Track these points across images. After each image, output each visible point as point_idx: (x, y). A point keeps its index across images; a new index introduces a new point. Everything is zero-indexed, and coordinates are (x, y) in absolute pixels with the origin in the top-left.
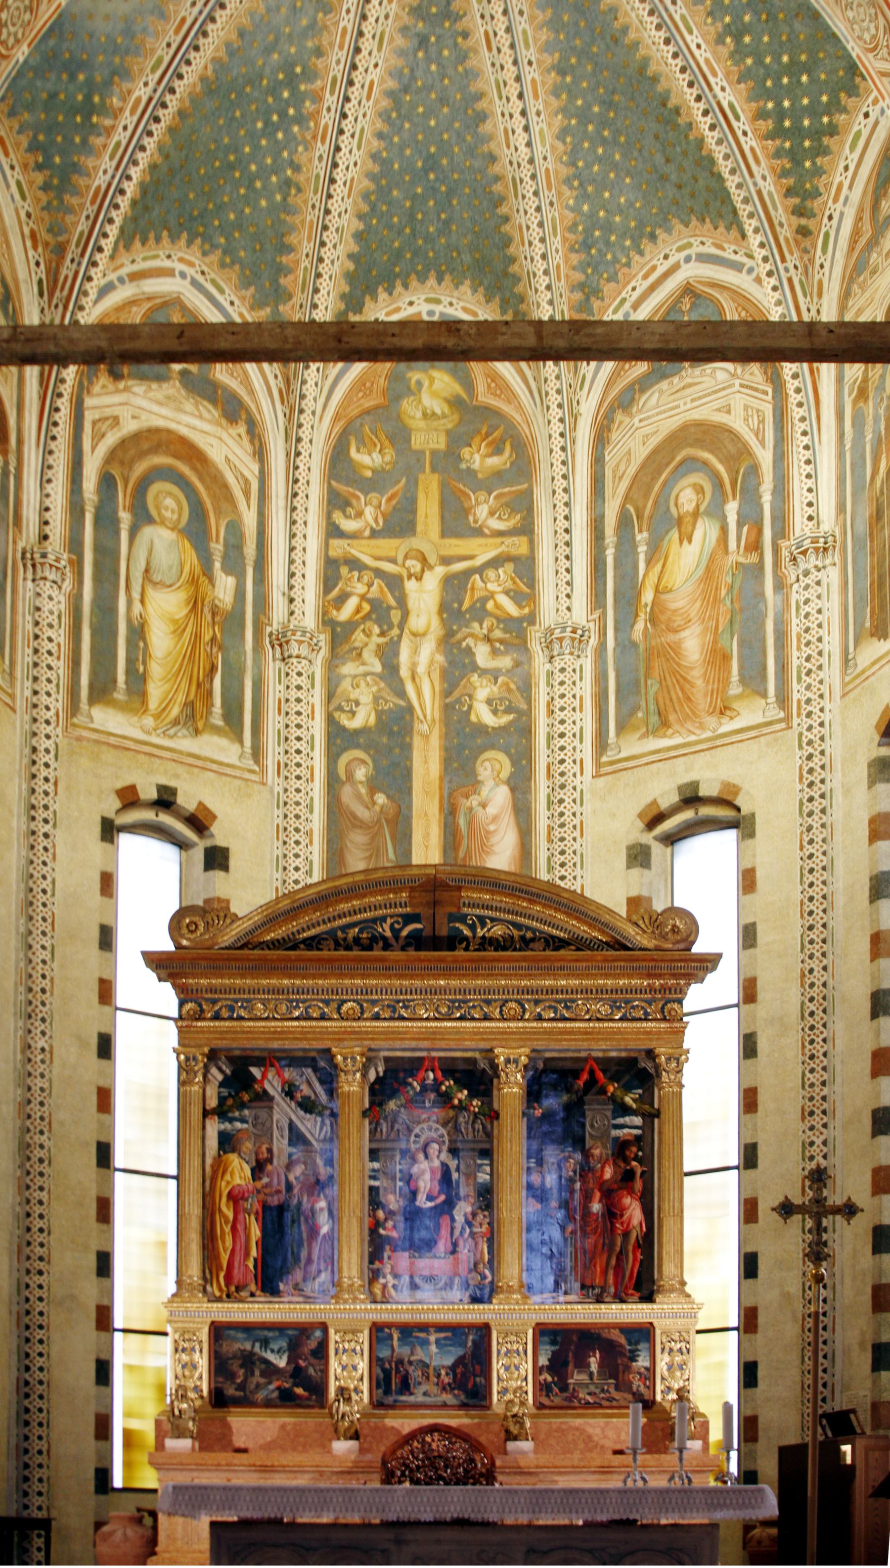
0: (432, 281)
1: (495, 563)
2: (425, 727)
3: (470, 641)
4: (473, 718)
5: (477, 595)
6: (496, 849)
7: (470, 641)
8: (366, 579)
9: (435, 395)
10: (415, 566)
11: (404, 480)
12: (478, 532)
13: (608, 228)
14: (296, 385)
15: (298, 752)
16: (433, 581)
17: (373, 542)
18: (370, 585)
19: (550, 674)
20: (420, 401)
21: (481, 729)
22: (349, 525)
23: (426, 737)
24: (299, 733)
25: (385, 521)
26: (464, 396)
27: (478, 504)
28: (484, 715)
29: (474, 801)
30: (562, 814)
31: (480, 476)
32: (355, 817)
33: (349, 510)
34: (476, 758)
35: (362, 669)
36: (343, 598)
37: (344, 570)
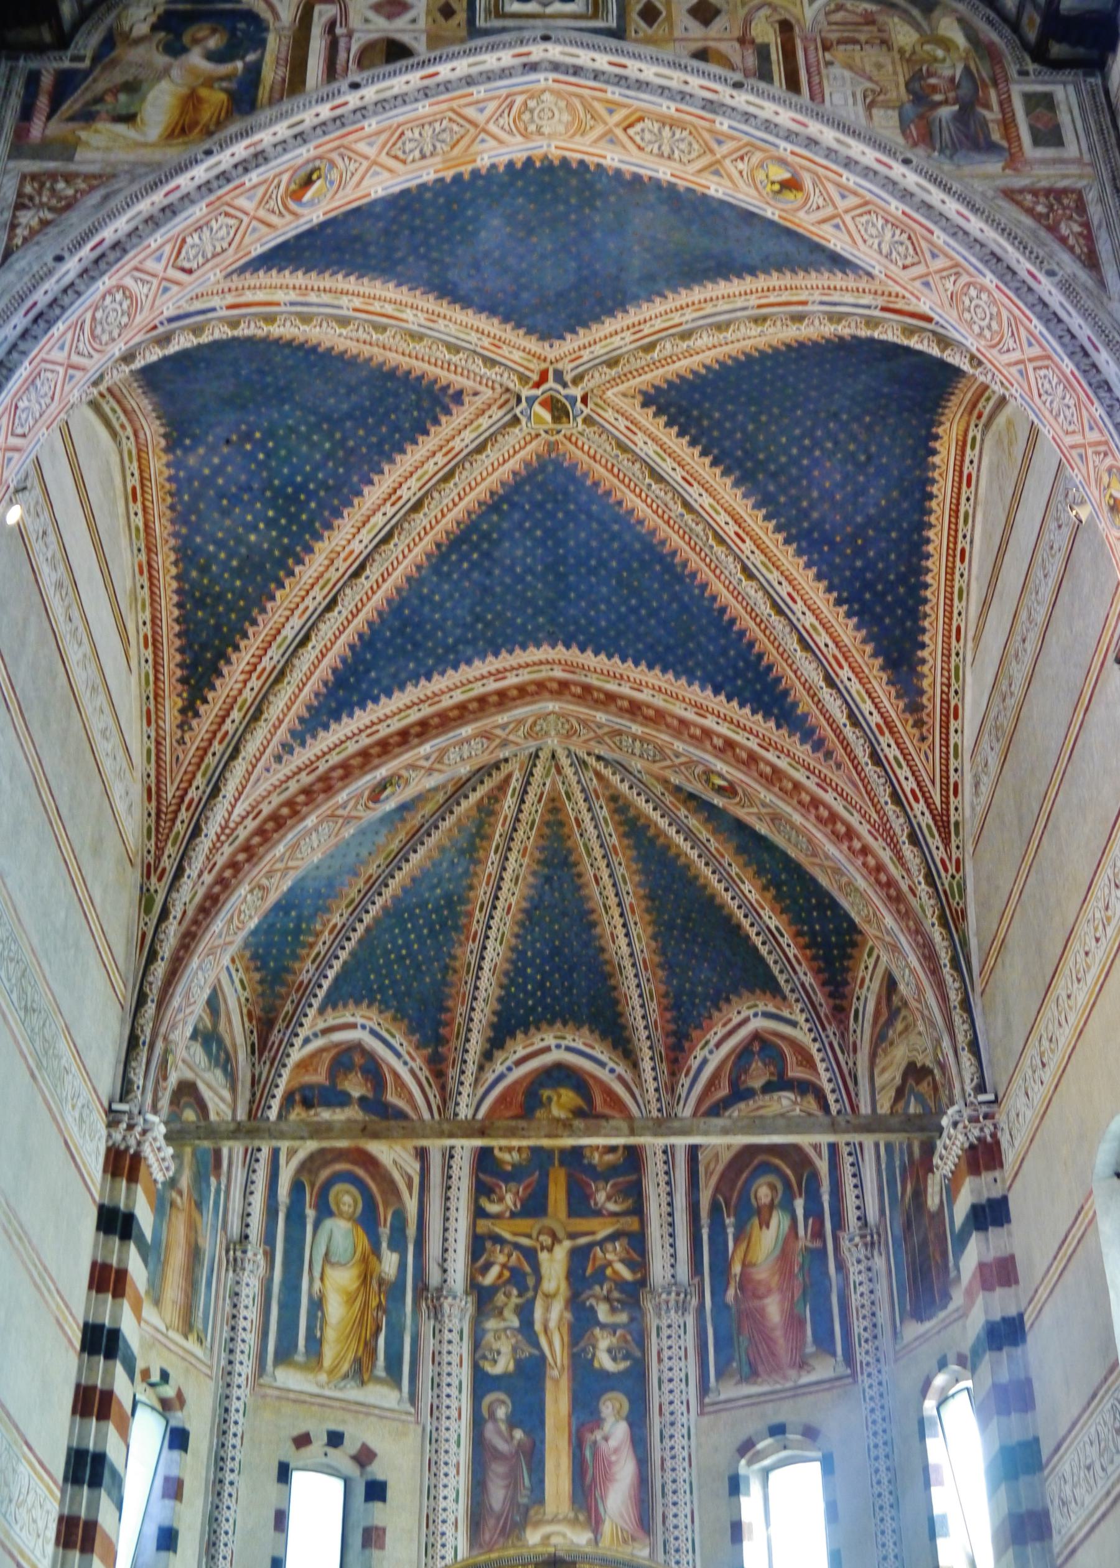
0: (559, 1025)
1: (613, 1238)
2: (555, 1373)
3: (592, 1301)
4: (596, 1364)
5: (598, 1263)
6: (618, 1477)
7: (592, 1301)
8: (506, 1251)
9: (560, 1106)
10: (546, 1240)
11: (537, 1173)
12: (598, 1213)
13: (692, 994)
14: (451, 1105)
15: (448, 1396)
16: (561, 1252)
17: (512, 1222)
18: (510, 1256)
19: (659, 1329)
20: (550, 1112)
21: (605, 1374)
22: (493, 1208)
23: (556, 1381)
24: (449, 1380)
25: (522, 1205)
26: (585, 1107)
27: (597, 1190)
28: (605, 1361)
29: (598, 1435)
30: (672, 1448)
31: (599, 1169)
32: (495, 1449)
33: (494, 1197)
34: (598, 1398)
35: (502, 1325)
36: (488, 1266)
37: (488, 1245)
